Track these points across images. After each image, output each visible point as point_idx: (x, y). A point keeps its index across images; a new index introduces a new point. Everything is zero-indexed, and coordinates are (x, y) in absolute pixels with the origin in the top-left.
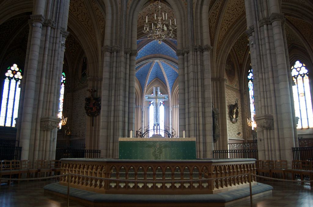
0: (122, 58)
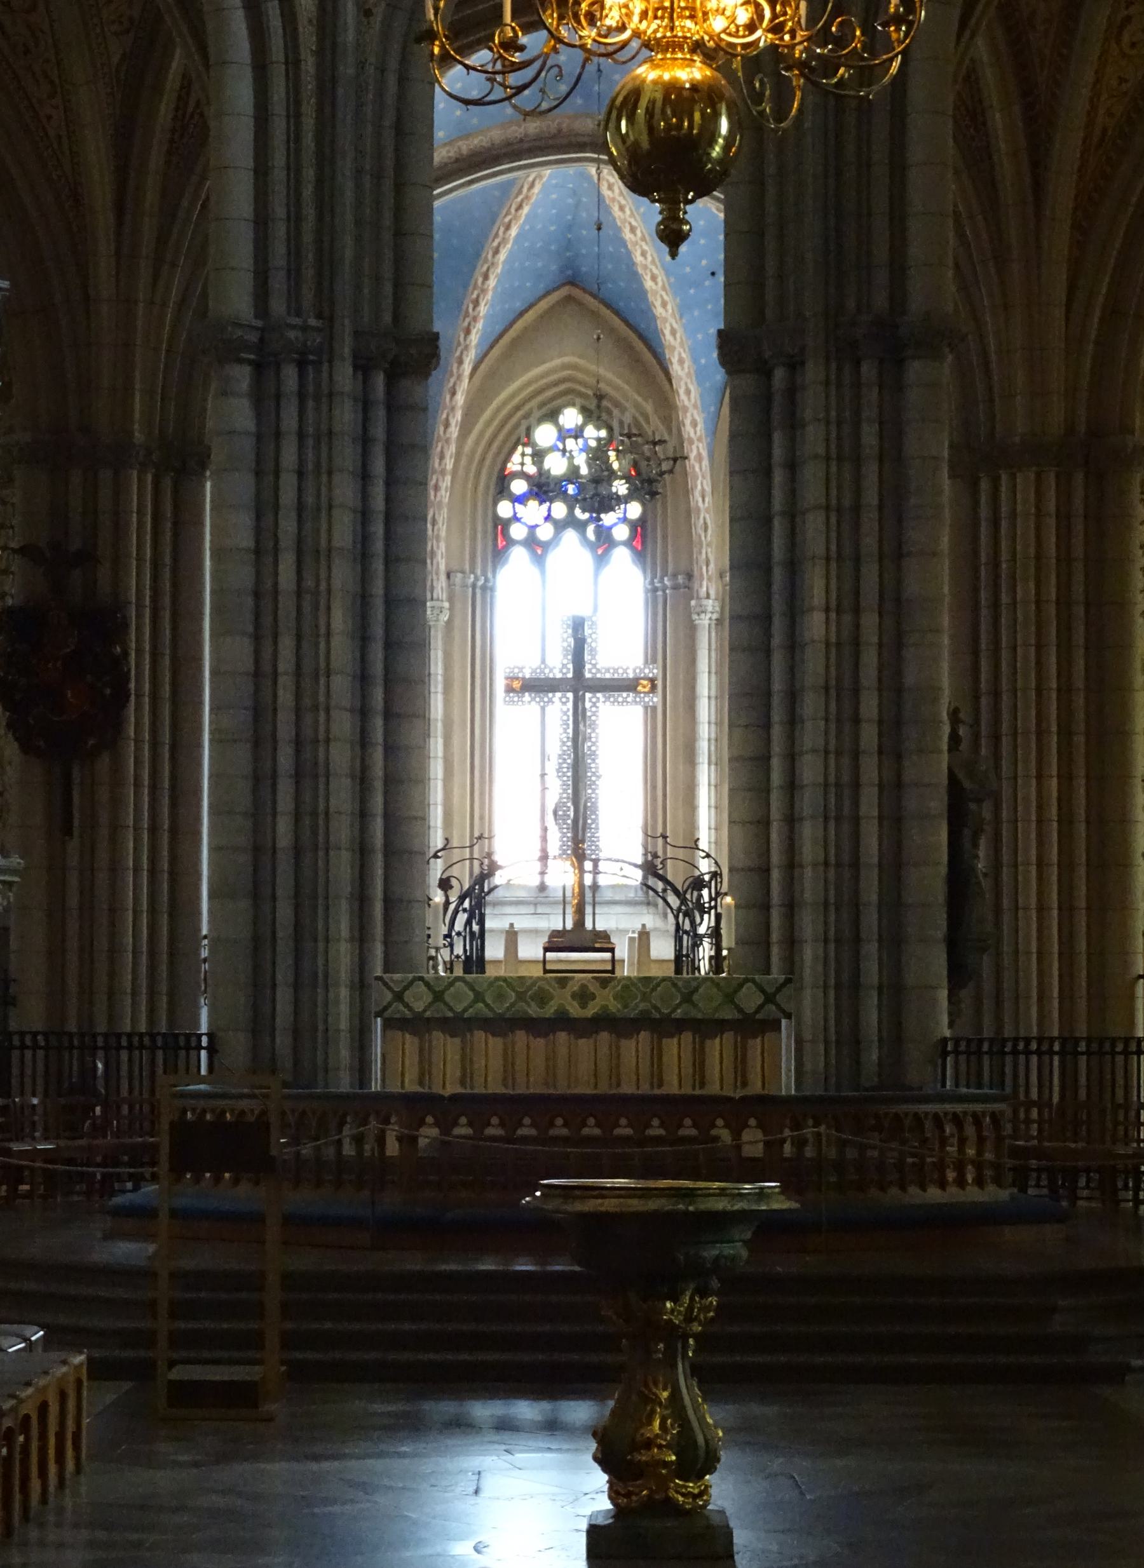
0: (336, 412)
